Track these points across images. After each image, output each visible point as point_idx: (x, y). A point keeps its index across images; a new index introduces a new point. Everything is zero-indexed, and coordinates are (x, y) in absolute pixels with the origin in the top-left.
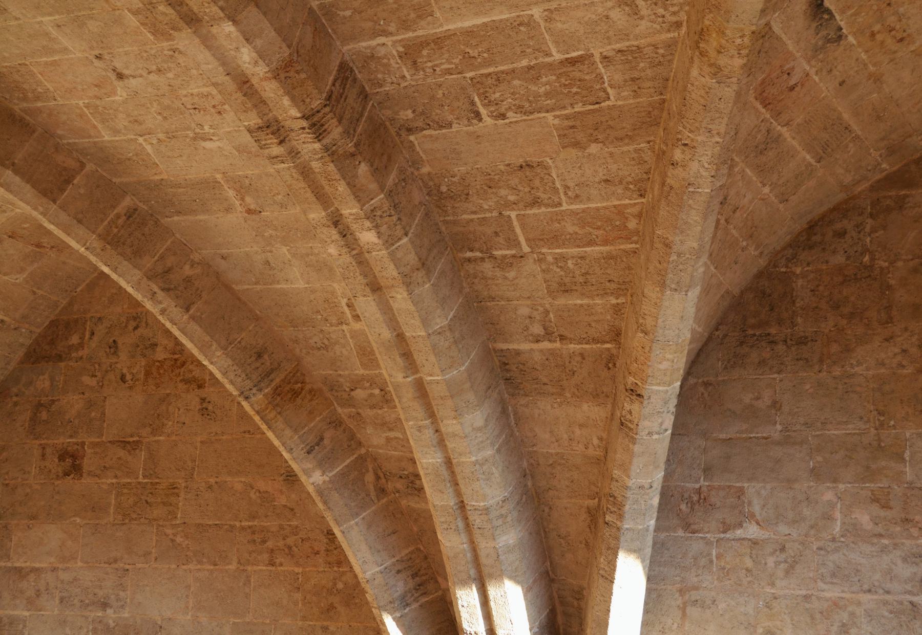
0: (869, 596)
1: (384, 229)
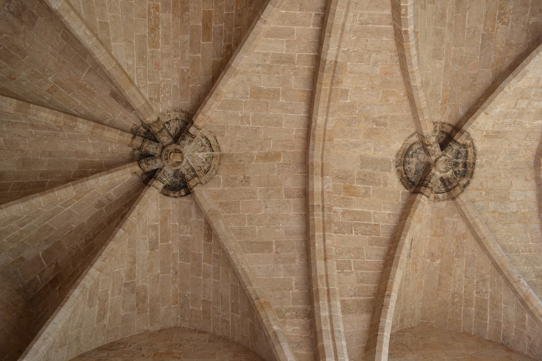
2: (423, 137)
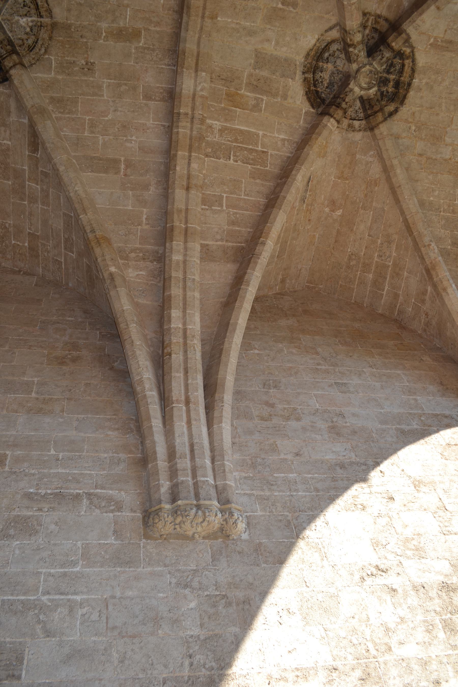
2: (346, 31)
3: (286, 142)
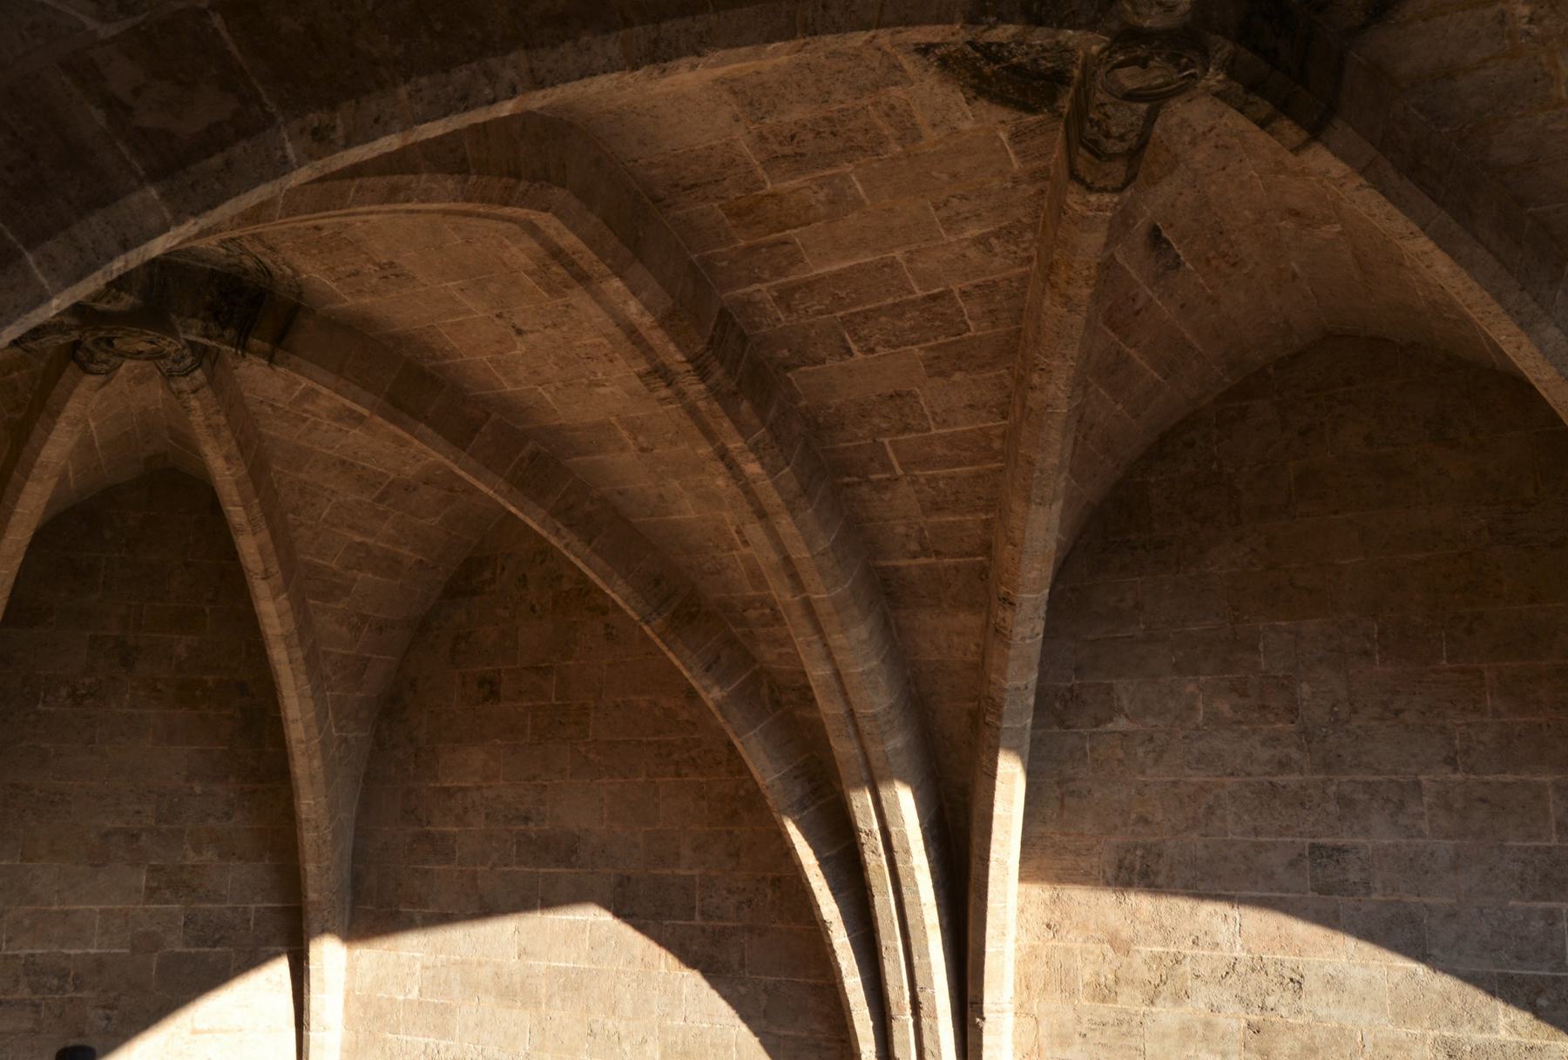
0: (1232, 779)
1: (767, 460)
3: (993, 241)
